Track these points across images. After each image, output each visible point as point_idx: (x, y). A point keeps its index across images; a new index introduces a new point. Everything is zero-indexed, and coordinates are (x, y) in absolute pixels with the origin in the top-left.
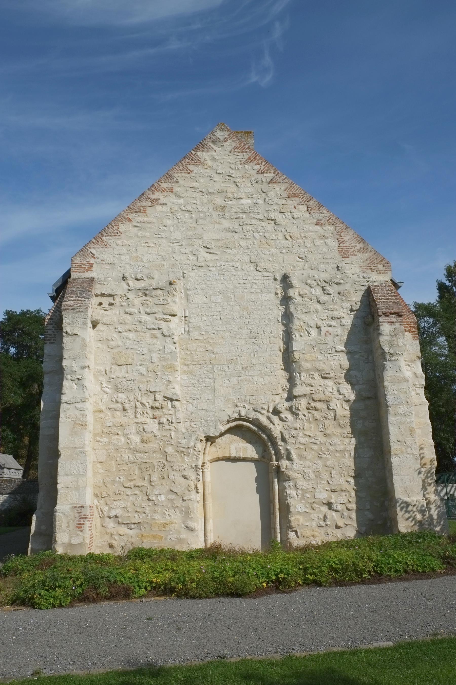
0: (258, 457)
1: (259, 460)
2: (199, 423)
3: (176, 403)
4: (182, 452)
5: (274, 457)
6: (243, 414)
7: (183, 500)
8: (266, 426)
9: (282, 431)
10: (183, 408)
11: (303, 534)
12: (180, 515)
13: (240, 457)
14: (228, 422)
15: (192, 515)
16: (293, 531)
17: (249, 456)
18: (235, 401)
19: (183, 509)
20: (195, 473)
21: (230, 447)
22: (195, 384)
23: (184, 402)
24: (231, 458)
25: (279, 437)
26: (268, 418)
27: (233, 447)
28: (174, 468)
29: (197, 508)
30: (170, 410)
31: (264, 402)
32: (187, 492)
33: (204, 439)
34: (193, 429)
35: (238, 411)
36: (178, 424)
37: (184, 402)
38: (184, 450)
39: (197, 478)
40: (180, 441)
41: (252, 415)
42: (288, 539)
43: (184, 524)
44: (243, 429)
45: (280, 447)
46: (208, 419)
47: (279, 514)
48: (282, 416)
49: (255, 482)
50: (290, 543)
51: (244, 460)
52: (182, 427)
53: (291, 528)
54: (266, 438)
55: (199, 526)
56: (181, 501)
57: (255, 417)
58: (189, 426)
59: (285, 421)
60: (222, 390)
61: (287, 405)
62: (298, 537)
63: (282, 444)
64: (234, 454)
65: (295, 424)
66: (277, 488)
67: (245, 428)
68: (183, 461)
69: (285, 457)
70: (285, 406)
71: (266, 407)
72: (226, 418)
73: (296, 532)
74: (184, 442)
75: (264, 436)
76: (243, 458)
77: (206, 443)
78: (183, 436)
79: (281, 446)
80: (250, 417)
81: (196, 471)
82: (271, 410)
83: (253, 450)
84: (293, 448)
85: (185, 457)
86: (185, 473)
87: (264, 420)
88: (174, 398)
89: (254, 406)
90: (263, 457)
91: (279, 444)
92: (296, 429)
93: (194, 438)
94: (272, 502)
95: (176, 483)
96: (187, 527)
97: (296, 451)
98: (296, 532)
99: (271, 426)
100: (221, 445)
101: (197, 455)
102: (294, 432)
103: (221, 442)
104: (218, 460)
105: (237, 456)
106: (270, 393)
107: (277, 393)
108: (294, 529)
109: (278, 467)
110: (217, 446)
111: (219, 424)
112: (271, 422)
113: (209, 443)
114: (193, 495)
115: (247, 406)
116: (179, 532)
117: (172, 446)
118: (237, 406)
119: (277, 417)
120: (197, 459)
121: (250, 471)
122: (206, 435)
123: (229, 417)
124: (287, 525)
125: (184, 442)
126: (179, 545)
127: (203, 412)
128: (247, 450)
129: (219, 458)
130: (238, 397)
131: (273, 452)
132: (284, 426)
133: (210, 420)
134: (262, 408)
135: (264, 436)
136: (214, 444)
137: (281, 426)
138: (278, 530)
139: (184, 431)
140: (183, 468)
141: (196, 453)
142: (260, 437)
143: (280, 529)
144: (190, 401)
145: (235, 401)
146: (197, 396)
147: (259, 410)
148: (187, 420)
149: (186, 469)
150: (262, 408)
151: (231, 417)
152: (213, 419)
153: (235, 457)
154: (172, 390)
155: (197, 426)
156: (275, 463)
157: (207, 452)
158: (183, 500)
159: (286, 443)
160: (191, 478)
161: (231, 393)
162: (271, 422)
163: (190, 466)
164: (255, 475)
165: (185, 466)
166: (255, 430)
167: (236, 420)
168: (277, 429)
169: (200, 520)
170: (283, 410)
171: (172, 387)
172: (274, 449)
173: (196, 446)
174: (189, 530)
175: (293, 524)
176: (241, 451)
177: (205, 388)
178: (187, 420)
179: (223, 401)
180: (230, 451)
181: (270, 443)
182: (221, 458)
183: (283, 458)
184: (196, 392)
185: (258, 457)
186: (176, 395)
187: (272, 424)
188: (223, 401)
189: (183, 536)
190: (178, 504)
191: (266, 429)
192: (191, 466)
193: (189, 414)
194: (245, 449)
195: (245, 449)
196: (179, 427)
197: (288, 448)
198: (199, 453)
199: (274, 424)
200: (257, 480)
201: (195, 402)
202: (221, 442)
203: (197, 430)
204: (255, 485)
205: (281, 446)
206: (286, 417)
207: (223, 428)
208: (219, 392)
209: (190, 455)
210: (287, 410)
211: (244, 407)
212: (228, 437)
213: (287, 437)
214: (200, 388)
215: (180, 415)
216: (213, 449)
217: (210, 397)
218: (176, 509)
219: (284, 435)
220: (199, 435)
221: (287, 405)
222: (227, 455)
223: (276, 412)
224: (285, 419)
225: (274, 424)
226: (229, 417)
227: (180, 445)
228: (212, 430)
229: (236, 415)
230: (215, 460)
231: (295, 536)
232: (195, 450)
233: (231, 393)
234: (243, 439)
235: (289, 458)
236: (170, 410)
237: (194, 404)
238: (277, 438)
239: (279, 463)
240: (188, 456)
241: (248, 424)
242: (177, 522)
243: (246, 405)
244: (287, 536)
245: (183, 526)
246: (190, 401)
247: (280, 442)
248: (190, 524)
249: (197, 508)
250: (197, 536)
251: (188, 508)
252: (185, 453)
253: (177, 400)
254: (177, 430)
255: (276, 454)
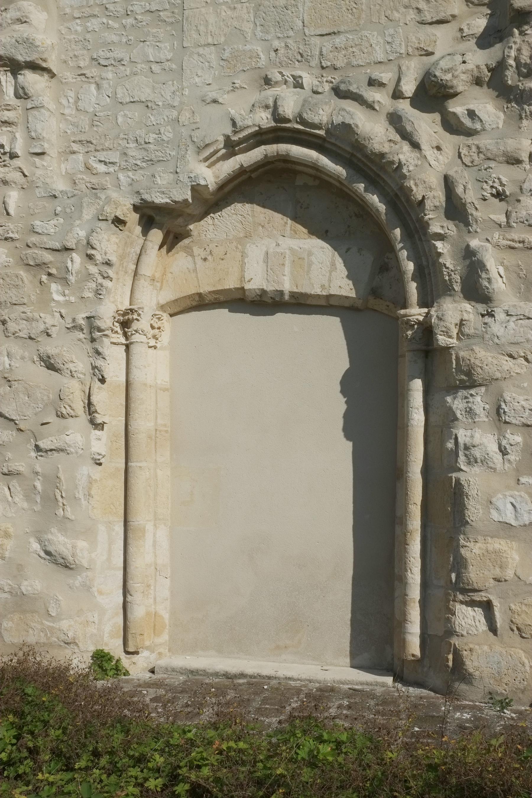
0: (353, 294)
1: (359, 304)
2: (114, 156)
3: (29, 78)
4: (41, 265)
5: (413, 288)
6: (289, 107)
7: (38, 448)
8: (382, 155)
9: (451, 173)
10: (64, 101)
11: (518, 620)
12: (25, 505)
13: (281, 293)
14: (232, 148)
15: (68, 508)
16: (472, 604)
17: (317, 290)
18: (263, 61)
19: (38, 485)
20: (88, 347)
21: (244, 255)
22: (111, 7)
23: (69, 76)
24: (250, 296)
25: (437, 197)
26: (395, 120)
27: (255, 252)
28: (12, 326)
29: (91, 481)
30: (8, 108)
31: (380, 56)
32: (51, 418)
33: (133, 218)
34: (94, 180)
35: (271, 103)
36: (37, 159)
37: (69, 76)
38: (48, 257)
39: (94, 368)
40: (37, 223)
41: (326, 112)
42: (451, 632)
43: (40, 541)
44: (300, 181)
45: (439, 245)
46: (152, 137)
47: (424, 526)
48: (457, 108)
49: (342, 392)
50: (457, 654)
51: (300, 304)
52: (55, 172)
53: (464, 591)
54: (382, 207)
55: (98, 551)
56: (33, 454)
57: (338, 120)
58: (82, 168)
59: (470, 133)
60: (212, 19)
61: (479, 59)
62: (493, 629)
63: (450, 228)
64: (256, 280)
65: (510, 141)
66: (417, 418)
67: (308, 174)
68: (45, 301)
69: (457, 287)
70: (470, 66)
71: (387, 76)
72: (218, 132)
73: (487, 607)
74: (50, 227)
75: (374, 199)
76: (293, 295)
77: (145, 232)
78: (49, 205)
79: (441, 237)
80: (316, 120)
81: (93, 340)
82: (409, 87)
83: (333, 264)
84: (497, 246)
85: (54, 287)
86: (50, 348)
87: (375, 131)
88: (20, 58)
89: (337, 78)
90: (375, 292)
91: (435, 228)
92: (514, 161)
93: (88, 214)
94: (397, 473)
95: (15, 385)
96: (48, 553)
97: (510, 258)
98: (487, 607)
99: (404, 154)
100: (212, 246)
101: (100, 280)
102: (505, 175)
103: (210, 235)
104: (201, 303)
105: (270, 288)
106: (412, 15)
107: (441, 16)
108: (477, 597)
109: (427, 330)
110: (196, 250)
111: (191, 155)
112: (406, 136)
113: (156, 235)
114: (75, 434)
115: (308, 80)
116: (20, 567)
117: (9, 244)
118: (267, 81)
119: (437, 117)
120: (97, 293)
121: (322, 350)
122: (136, 200)
123: (234, 124)
124: (447, 580)
125: (50, 227)
126: (16, 617)
127: (135, 113)
128: (310, 264)
129: (200, 295)
130: (276, 44)
131: (410, 267)
132: (464, 151)
133: (160, 142)
134: (372, 83)
135: (374, 199)
136: (186, 241)
137: (449, 151)
138: (415, 592)
139: (60, 185)
140: (42, 327)
141: (93, 269)
142: (364, 211)
143: (425, 585)
144: (93, 72)
145: (263, 61)
146: (119, 53)
147: (353, 88)
148: (75, 147)
149: (53, 331)
150: (372, 83)
151: (240, 123)
152: (168, 134)
153: (264, 292)
154: (17, 27)
155: (111, 170)
156: (416, 313)
157: (146, 269)
158: (38, 448)
159: (467, 224)
160: (71, 366)
161: (248, 28)
162: (406, 136)
163: (69, 320)
164: (343, 363)
165: (50, 320)
166: (338, 178)
167: (261, 137)
168: (429, 162)
169: (102, 528)
170: (461, 84)
171: (18, 14)
172: (416, 256)
173: (94, 241)
174: (55, 562)
175: (474, 574)
176: (287, 269)
177: (148, 18)
178: (75, 147)
179: (214, 64)
180: (243, 270)
181: (398, 232)
182: (211, 298)
183: (447, 289)
184: (115, 38)
185: (353, 294)
186: (28, 43)
187: (406, 147)
188: (214, 64)
189: (33, 584)
190: (20, 466)
191: (382, 168)
192: (74, 320)
193: (85, 121)
194: (301, 261)
195: (301, 261)
196: (39, 172)
197: (474, 243)
198: (105, 268)
199: (416, 146)
200: (348, 384)
201: (110, 75)
202: (210, 235)
203: (108, 181)
204: (340, 405)
205: (441, 237)
206: (471, 114)
207: (210, 176)
208: (202, 28)
209: (72, 279)
210: (478, 82)
211: (298, 84)
212: (240, 214)
213: (469, 194)
214: (130, 21)
215: (50, 128)
216: (180, 260)
217: (166, 54)
218: (14, 483)
219: (459, 190)
220: (108, 200)
221: (479, 59)
222: (231, 283)
223: (433, 95)
224: (467, 122)
225: (416, 146)
226: (234, 124)
227: (34, 239)
228: (164, 179)
229: (264, 119)
230: (189, 303)
231: (482, 626)
232: (90, 257)
233: (248, 28)
234: (295, 218)
235: (476, 291)
236: (8, 108)
237: (105, 84)
238: (428, 204)
239: (433, 312)
240: (64, 281)
241: (312, 154)
242: (11, 530)
243: (304, 74)
244: (448, 620)
245: (36, 546)
246: (93, 72)
247: (438, 224)
248: (60, 542)
249: (91, 481)
250: (87, 588)
251: (53, 481)
252: (53, 271)
253: (34, 67)
254: (28, 185)
255: (421, 275)
